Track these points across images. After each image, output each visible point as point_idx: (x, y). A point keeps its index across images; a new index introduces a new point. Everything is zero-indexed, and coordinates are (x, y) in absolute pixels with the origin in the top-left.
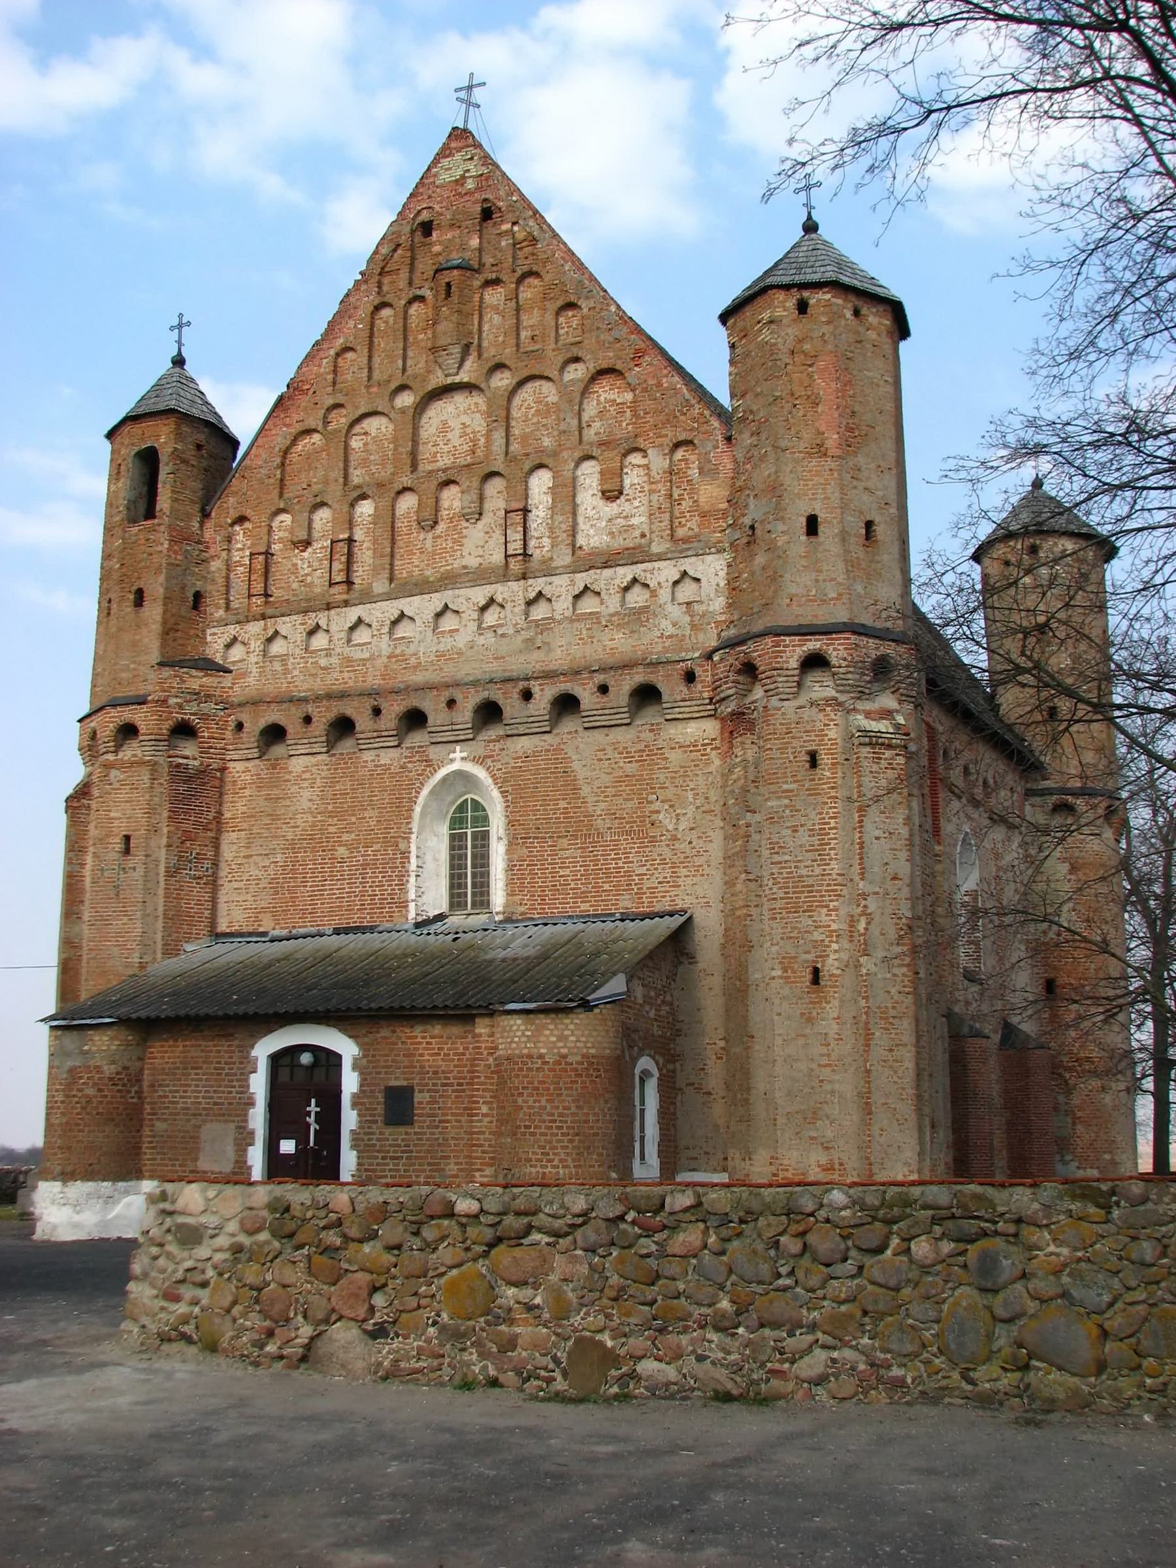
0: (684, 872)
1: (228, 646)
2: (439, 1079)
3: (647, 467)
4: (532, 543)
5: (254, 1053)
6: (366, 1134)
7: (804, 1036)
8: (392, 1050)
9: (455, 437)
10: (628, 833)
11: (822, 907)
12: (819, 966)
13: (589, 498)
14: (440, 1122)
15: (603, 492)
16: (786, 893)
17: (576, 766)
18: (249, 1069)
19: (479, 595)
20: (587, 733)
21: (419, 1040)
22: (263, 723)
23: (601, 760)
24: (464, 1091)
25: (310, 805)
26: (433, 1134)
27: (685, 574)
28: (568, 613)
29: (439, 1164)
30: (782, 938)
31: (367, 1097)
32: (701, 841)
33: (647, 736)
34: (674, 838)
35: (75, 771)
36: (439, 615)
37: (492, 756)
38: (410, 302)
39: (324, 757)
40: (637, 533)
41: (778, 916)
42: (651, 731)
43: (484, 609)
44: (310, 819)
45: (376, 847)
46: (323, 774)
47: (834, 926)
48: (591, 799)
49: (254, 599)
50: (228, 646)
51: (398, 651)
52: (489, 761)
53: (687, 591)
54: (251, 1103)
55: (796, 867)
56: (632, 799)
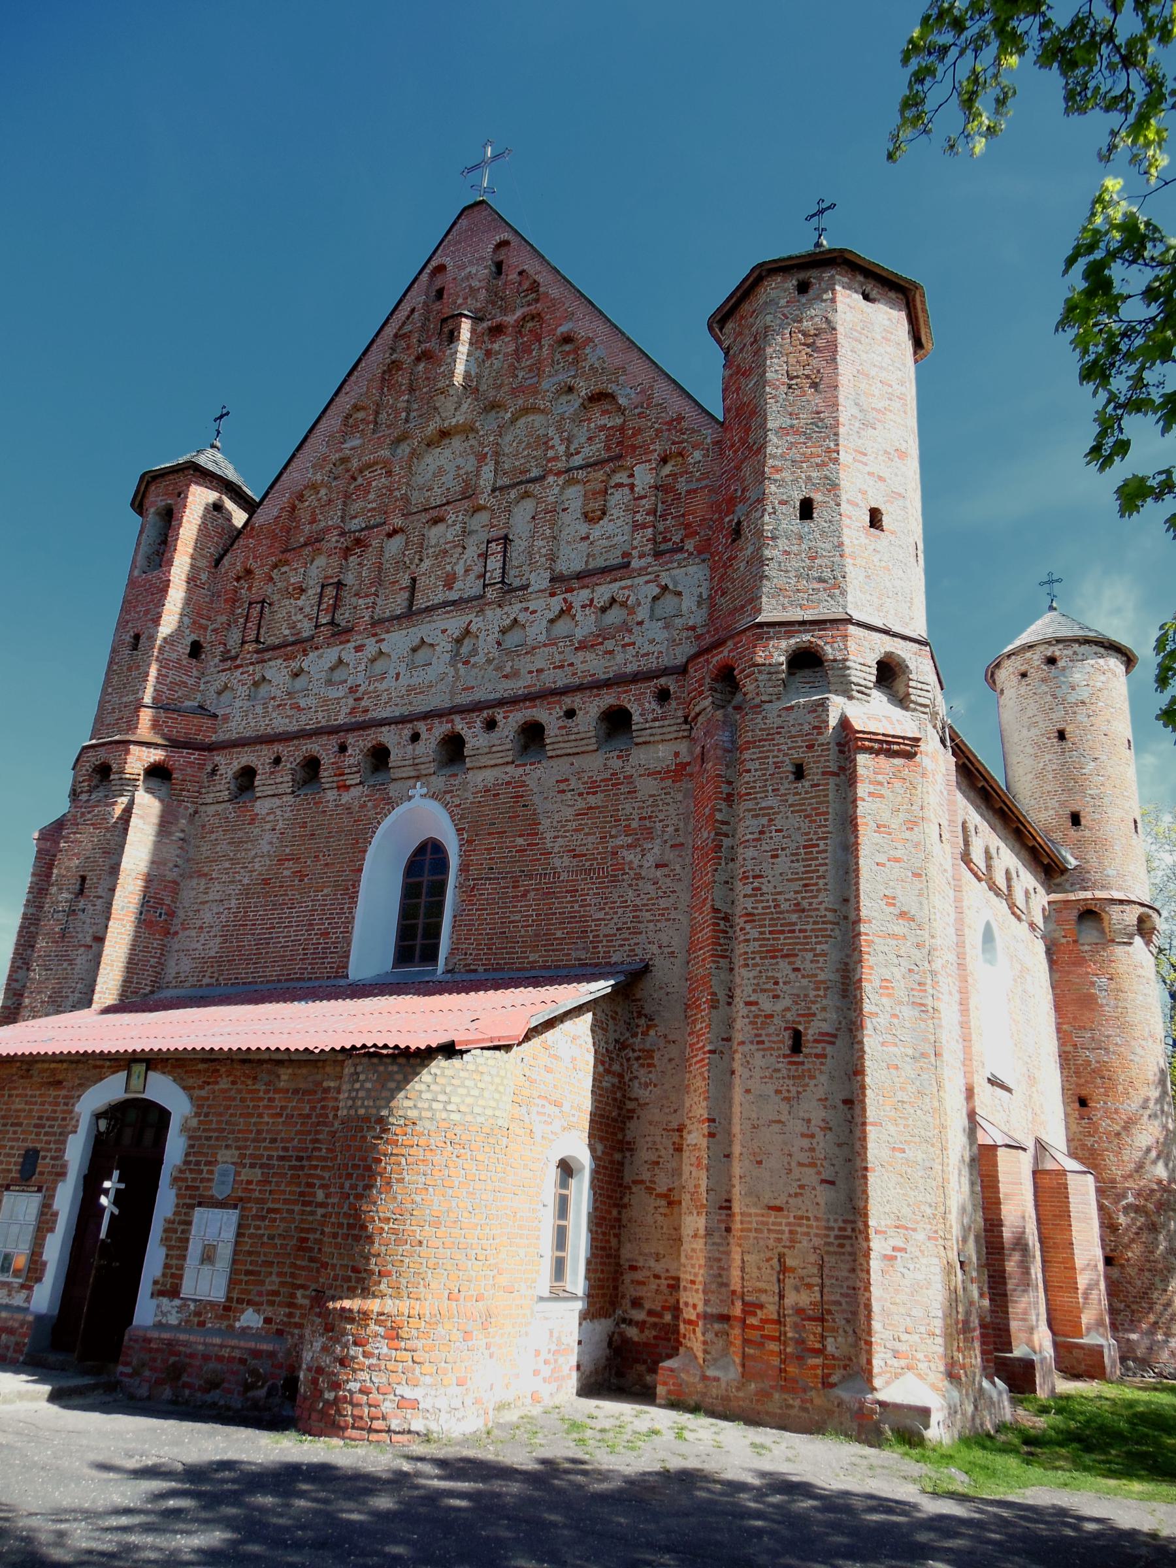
1: (219, 693)
2: (277, 1149)
3: (632, 487)
4: (512, 573)
5: (77, 1109)
6: (180, 1223)
7: (779, 1122)
8: (228, 1107)
9: (448, 480)
10: (587, 872)
11: (806, 950)
12: (801, 1028)
13: (572, 525)
14: (270, 1211)
15: (585, 515)
16: (761, 933)
17: (536, 799)
18: (70, 1128)
19: (454, 623)
20: (552, 762)
21: (261, 1094)
22: (236, 766)
23: (563, 791)
24: (302, 1168)
25: (268, 847)
26: (259, 1228)
27: (665, 588)
28: (542, 638)
29: (258, 1273)
30: (754, 991)
31: (191, 1171)
32: (668, 880)
33: (616, 764)
34: (638, 877)
36: (414, 650)
37: (452, 791)
38: (418, 359)
39: (289, 799)
40: (619, 553)
41: (750, 962)
42: (619, 757)
43: (459, 641)
44: (268, 862)
45: (325, 891)
46: (286, 815)
47: (822, 976)
48: (548, 835)
49: (246, 646)
50: (219, 693)
51: (371, 688)
52: (448, 797)
54: (62, 1175)
55: (774, 900)
56: (595, 834)
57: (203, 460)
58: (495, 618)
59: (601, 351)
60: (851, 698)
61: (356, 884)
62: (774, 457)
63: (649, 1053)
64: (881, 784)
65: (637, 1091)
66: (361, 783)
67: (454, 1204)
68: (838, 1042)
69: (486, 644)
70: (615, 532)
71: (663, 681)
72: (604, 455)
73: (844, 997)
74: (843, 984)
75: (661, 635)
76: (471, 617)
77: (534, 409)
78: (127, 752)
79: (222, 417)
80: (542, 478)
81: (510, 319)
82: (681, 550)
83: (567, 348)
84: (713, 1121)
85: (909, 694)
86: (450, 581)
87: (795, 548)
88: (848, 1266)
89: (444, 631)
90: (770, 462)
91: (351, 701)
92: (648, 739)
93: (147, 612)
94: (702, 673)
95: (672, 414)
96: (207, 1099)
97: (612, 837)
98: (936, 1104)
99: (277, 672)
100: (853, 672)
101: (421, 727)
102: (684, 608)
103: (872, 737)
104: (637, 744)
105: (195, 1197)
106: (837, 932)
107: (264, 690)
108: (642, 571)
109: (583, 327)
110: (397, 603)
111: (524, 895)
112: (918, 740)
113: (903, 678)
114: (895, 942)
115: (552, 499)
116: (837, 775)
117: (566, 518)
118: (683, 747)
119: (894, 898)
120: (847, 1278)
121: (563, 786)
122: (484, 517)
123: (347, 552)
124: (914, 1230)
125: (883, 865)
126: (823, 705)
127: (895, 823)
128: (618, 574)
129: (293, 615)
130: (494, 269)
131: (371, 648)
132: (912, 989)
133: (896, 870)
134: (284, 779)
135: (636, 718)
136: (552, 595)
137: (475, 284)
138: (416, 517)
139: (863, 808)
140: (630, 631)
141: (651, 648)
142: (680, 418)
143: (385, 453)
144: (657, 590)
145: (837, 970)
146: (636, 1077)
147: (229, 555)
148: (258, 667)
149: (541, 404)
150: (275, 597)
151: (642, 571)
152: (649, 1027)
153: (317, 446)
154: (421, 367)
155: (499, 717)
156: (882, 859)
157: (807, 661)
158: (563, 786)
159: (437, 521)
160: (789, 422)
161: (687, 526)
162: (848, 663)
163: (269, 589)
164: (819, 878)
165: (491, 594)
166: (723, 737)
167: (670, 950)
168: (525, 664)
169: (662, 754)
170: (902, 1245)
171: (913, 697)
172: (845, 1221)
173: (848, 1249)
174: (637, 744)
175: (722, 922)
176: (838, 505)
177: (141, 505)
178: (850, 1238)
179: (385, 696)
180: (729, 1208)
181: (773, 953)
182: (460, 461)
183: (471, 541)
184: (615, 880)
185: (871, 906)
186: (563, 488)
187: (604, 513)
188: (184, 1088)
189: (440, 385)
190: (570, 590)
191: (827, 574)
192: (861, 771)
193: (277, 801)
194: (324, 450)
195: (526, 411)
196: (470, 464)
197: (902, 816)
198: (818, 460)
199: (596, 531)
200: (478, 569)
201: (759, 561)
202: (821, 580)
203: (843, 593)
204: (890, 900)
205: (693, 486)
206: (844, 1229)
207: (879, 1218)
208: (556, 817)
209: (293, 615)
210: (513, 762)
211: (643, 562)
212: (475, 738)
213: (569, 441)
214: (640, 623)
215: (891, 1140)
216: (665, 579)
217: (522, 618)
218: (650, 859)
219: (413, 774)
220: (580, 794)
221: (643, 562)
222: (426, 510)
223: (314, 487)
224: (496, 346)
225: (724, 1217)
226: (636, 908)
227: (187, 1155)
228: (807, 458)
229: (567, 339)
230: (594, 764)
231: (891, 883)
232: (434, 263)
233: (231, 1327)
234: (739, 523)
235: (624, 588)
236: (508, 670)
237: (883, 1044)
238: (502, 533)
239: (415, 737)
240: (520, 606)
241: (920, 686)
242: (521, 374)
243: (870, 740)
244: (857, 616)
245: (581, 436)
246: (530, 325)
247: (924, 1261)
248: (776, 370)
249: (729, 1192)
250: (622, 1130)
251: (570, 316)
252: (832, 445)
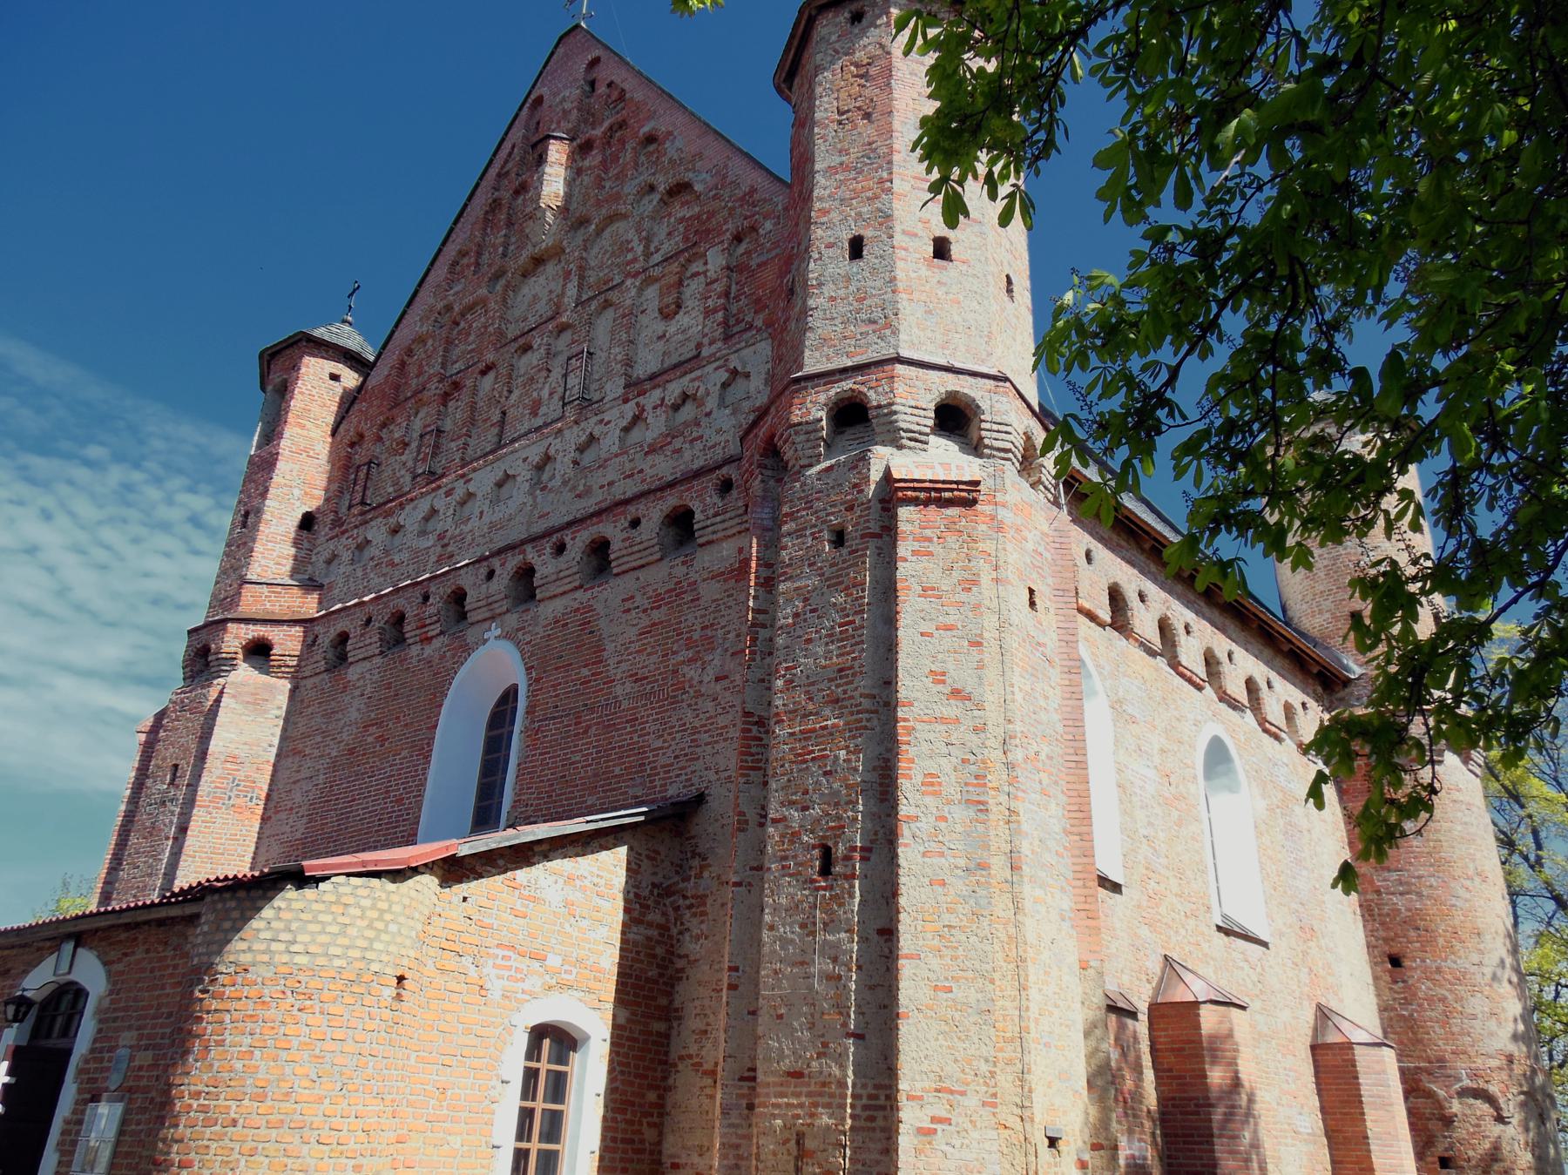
0: (705, 737)
1: (329, 562)
4: (594, 386)
12: (830, 844)
13: (650, 324)
15: (661, 311)
17: (603, 623)
20: (619, 581)
22: (333, 633)
23: (629, 610)
28: (615, 449)
32: (727, 694)
33: (680, 571)
34: (698, 694)
39: (378, 660)
42: (684, 563)
45: (404, 753)
57: (320, 332)
59: (678, 144)
60: (900, 447)
61: (430, 744)
62: (820, 199)
63: (702, 899)
64: (930, 540)
65: (690, 947)
66: (442, 633)
67: (288, 1070)
68: (873, 857)
69: (563, 465)
71: (724, 470)
72: (682, 246)
73: (882, 801)
74: (881, 785)
78: (225, 630)
81: (598, 132)
83: (651, 148)
84: (736, 969)
85: (981, 439)
87: (842, 293)
88: (879, 1146)
89: (525, 460)
90: (817, 205)
91: (439, 549)
92: (710, 537)
94: (753, 452)
96: (122, 973)
97: (674, 653)
98: (1012, 930)
100: (900, 417)
101: (496, 563)
102: (752, 389)
103: (916, 484)
104: (701, 545)
106: (875, 722)
108: (713, 358)
111: (586, 732)
112: (977, 483)
113: (976, 421)
114: (944, 727)
115: (628, 302)
116: (879, 536)
117: (644, 319)
119: (943, 674)
120: (878, 1162)
121: (628, 605)
122: (567, 337)
123: (445, 398)
124: (963, 1093)
125: (930, 635)
126: (863, 459)
127: (946, 584)
130: (587, 88)
131: (460, 492)
132: (966, 784)
133: (948, 640)
136: (626, 401)
137: (567, 106)
139: (903, 570)
140: (698, 424)
142: (753, 191)
143: (483, 291)
144: (726, 375)
145: (874, 769)
146: (688, 930)
148: (361, 529)
149: (622, 209)
151: (713, 358)
152: (702, 867)
153: (426, 297)
155: (567, 539)
156: (925, 627)
157: (853, 417)
158: (628, 605)
159: (527, 348)
160: (838, 160)
162: (894, 408)
163: (378, 449)
164: (854, 659)
167: (727, 774)
170: (944, 1114)
171: (986, 441)
172: (876, 1087)
173: (880, 1123)
174: (701, 545)
175: (754, 728)
176: (891, 237)
178: (883, 1108)
179: (469, 537)
180: (754, 1079)
184: (675, 701)
185: (911, 684)
186: (641, 290)
187: (679, 307)
188: (105, 964)
189: (528, 210)
190: (642, 393)
192: (903, 527)
193: (367, 664)
194: (431, 300)
195: (611, 219)
197: (957, 575)
198: (870, 194)
199: (672, 330)
203: (895, 332)
204: (939, 677)
205: (764, 258)
206: (876, 1097)
207: (913, 1080)
208: (620, 640)
210: (581, 587)
211: (714, 348)
212: (545, 566)
214: (708, 414)
215: (931, 975)
216: (734, 362)
219: (487, 615)
220: (645, 611)
221: (714, 348)
223: (421, 340)
224: (587, 163)
225: (745, 1091)
226: (695, 731)
227: (95, 1041)
228: (857, 194)
229: (651, 139)
230: (658, 576)
231: (940, 656)
232: (533, 97)
235: (693, 380)
237: (924, 855)
239: (491, 575)
240: (595, 419)
241: (995, 427)
242: (608, 184)
243: (914, 489)
244: (905, 353)
245: (661, 231)
247: (975, 1135)
248: (825, 109)
249: (753, 1059)
250: (669, 994)
251: (651, 115)
252: (885, 175)
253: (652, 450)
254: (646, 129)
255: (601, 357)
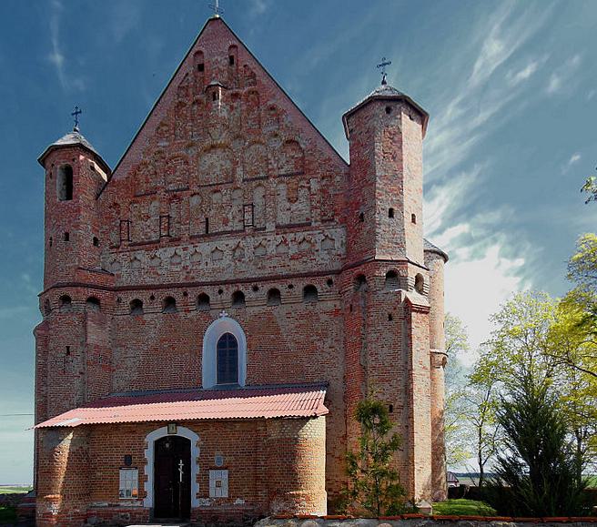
3: (309, 188)
4: (256, 221)
15: (289, 199)
19: (232, 242)
35: (39, 319)
36: (213, 252)
38: (194, 103)
43: (234, 250)
53: (329, 243)
58: (251, 242)
69: (248, 253)
70: (302, 208)
71: (330, 276)
72: (295, 171)
75: (327, 257)
76: (240, 240)
77: (259, 142)
79: (77, 113)
80: (267, 178)
82: (332, 220)
83: (272, 112)
86: (226, 222)
93: (70, 222)
94: (350, 275)
95: (326, 156)
99: (142, 255)
101: (223, 287)
105: (207, 467)
107: (136, 264)
108: (317, 228)
109: (281, 104)
110: (201, 230)
115: (272, 189)
118: (338, 303)
122: (239, 193)
128: (307, 228)
129: (146, 229)
134: (158, 306)
135: (319, 290)
138: (204, 188)
141: (323, 262)
142: (330, 160)
147: (103, 194)
149: (262, 139)
150: (133, 219)
153: (143, 142)
154: (195, 108)
157: (392, 275)
159: (215, 192)
161: (335, 210)
165: (248, 230)
166: (362, 302)
168: (268, 264)
169: (330, 305)
177: (44, 161)
181: (383, 380)
182: (223, 163)
183: (234, 203)
189: (212, 122)
190: (285, 233)
191: (399, 242)
192: (413, 318)
196: (228, 165)
199: (294, 208)
200: (239, 217)
201: (373, 233)
202: (397, 244)
203: (405, 250)
209: (146, 229)
211: (317, 224)
213: (278, 161)
214: (317, 251)
217: (264, 243)
218: (327, 345)
222: (210, 185)
224: (235, 105)
229: (272, 108)
230: (302, 307)
233: (231, 505)
234: (362, 215)
236: (260, 265)
238: (250, 202)
242: (250, 122)
246: (252, 96)
253: (293, 258)
254: (270, 103)
255: (258, 209)
